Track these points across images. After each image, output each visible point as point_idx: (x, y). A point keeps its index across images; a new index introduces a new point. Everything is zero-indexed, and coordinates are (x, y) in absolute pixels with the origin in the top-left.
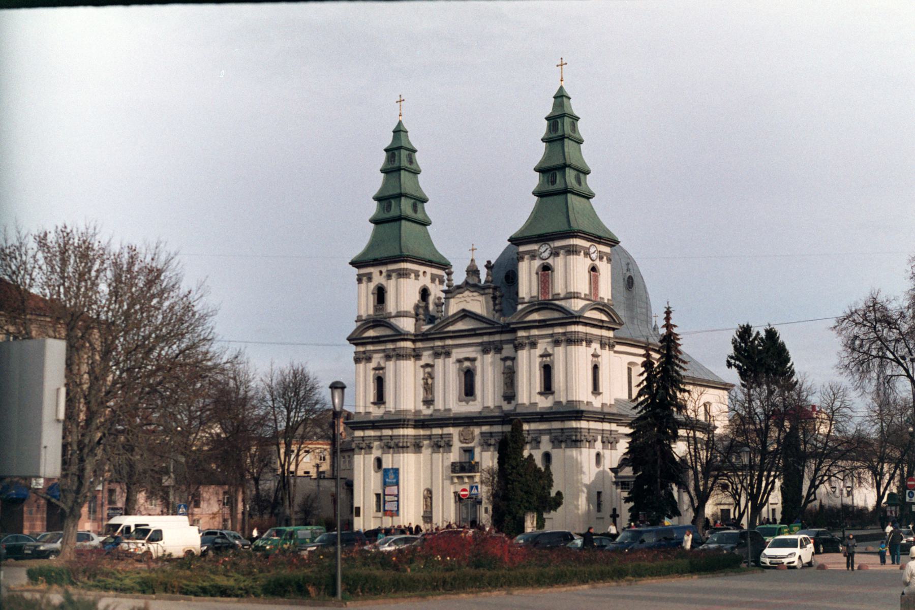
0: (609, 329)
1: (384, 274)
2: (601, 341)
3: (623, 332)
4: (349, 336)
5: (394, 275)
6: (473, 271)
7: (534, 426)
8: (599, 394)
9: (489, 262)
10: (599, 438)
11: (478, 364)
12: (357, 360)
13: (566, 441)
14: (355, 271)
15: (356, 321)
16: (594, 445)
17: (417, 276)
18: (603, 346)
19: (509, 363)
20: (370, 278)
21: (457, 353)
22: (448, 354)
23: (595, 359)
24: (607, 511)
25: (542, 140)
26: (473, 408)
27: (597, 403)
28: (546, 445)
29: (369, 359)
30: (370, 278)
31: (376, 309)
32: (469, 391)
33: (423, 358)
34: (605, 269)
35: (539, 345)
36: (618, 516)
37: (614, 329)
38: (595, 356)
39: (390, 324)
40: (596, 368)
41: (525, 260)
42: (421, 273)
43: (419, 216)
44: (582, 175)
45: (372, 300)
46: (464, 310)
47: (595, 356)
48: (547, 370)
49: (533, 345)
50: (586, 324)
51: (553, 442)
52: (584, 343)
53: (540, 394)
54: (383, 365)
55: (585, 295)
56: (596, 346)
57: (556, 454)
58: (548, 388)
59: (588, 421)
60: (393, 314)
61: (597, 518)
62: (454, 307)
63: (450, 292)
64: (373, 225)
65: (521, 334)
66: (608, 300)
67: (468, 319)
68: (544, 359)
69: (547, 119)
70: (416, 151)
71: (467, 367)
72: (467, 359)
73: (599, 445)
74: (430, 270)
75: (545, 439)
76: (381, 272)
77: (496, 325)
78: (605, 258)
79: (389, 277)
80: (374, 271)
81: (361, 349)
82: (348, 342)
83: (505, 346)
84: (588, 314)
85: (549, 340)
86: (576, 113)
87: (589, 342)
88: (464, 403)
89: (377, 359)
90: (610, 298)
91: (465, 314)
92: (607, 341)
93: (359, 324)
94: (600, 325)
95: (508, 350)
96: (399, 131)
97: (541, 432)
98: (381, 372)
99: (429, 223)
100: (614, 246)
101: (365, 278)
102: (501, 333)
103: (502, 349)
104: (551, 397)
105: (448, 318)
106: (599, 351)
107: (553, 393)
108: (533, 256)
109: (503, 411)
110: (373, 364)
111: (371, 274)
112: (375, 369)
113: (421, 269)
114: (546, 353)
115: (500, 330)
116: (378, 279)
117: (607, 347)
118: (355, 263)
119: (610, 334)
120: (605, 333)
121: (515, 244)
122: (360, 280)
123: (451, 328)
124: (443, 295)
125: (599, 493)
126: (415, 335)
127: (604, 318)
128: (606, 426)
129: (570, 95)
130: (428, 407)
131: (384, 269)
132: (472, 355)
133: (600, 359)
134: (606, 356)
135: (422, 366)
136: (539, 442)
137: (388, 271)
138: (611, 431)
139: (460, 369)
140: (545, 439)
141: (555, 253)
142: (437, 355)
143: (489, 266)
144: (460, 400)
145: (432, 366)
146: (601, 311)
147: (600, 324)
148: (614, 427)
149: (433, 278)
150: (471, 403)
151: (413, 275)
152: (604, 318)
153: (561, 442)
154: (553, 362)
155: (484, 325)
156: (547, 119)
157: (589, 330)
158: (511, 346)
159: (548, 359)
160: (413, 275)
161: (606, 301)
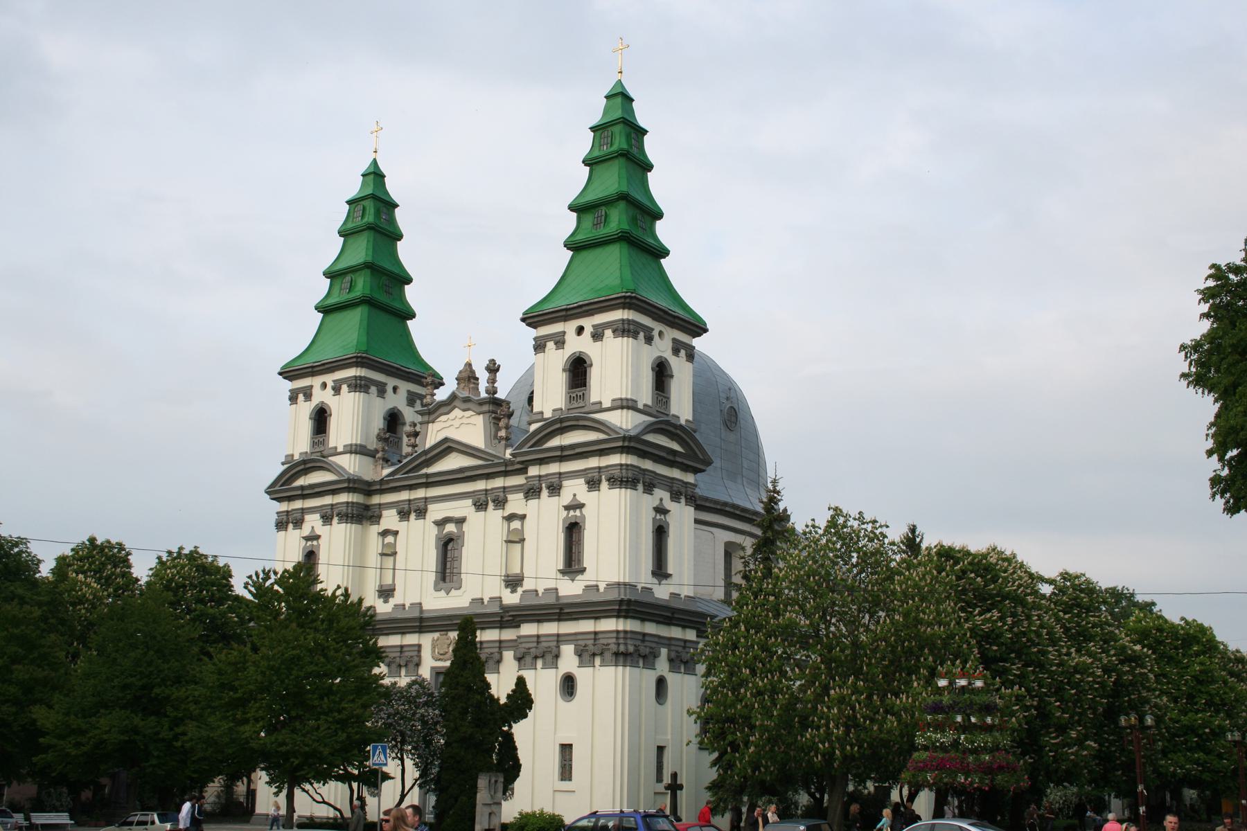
0: (686, 468)
1: (330, 384)
2: (671, 487)
3: (707, 484)
4: (269, 488)
5: (345, 388)
6: (468, 377)
7: (550, 628)
8: (668, 576)
9: (493, 361)
10: (664, 651)
11: (465, 527)
12: (281, 525)
13: (601, 654)
14: (289, 385)
15: (283, 464)
16: (653, 664)
17: (382, 392)
18: (675, 497)
19: (516, 524)
20: (308, 396)
21: (437, 511)
22: (422, 513)
23: (658, 517)
24: (667, 779)
25: (583, 162)
26: (457, 601)
27: (662, 592)
28: (568, 660)
29: (298, 523)
30: (308, 396)
31: (314, 444)
32: (447, 572)
33: (382, 521)
34: (682, 372)
35: (563, 492)
36: (681, 787)
37: (696, 471)
38: (661, 510)
39: (330, 465)
40: (660, 533)
41: (546, 350)
42: (389, 389)
43: (397, 305)
44: (648, 219)
45: (306, 427)
46: (446, 440)
47: (661, 510)
48: (573, 530)
49: (555, 489)
50: (643, 454)
51: (580, 656)
52: (640, 487)
53: (563, 572)
54: (318, 533)
55: (645, 405)
56: (661, 495)
57: (583, 676)
58: (572, 564)
59: (643, 620)
60: (340, 449)
61: (655, 793)
62: (434, 434)
63: (433, 411)
64: (321, 315)
65: (533, 471)
66: (687, 421)
67: (454, 455)
68: (572, 513)
69: (590, 128)
70: (397, 206)
71: (450, 533)
72: (447, 520)
73: (662, 666)
74: (405, 387)
75: (568, 650)
76: (324, 385)
77: (496, 461)
78: (683, 353)
79: (337, 390)
80: (316, 382)
81: (284, 507)
82: (268, 497)
83: (510, 497)
84: (651, 438)
85: (582, 481)
86: (642, 122)
87: (649, 489)
88: (443, 593)
89: (313, 522)
90: (691, 419)
91: (447, 447)
92: (683, 490)
93: (286, 466)
94: (668, 459)
95: (516, 503)
96: (375, 175)
97: (560, 639)
98: (315, 543)
99: (412, 316)
100: (699, 335)
101: (301, 397)
102: (506, 474)
103: (505, 501)
104: (580, 577)
105: (425, 452)
106: (668, 504)
107: (583, 571)
108: (560, 342)
109: (502, 607)
110: (306, 530)
111: (311, 387)
112: (307, 539)
113: (391, 382)
114: (574, 503)
115: (503, 469)
116: (319, 396)
117: (683, 500)
118: (289, 373)
119: (690, 478)
120: (676, 473)
121: (529, 325)
122: (293, 399)
123: (424, 471)
124: (419, 418)
125: (661, 749)
126: (369, 484)
127: (675, 446)
128: (676, 632)
129: (632, 95)
130: (386, 601)
131: (329, 379)
132: (457, 514)
133: (667, 516)
134: (682, 516)
135: (379, 533)
136: (557, 656)
137: (334, 381)
138: (685, 641)
139: (438, 538)
140: (568, 650)
141: (597, 336)
142: (404, 515)
143: (493, 369)
144: (437, 589)
145: (396, 533)
146: (672, 436)
147: (671, 458)
148: (691, 635)
149: (412, 399)
150: (453, 592)
151: (373, 389)
152: (675, 446)
153: (594, 655)
154: (583, 517)
155: (480, 462)
156: (590, 128)
157: (648, 465)
158: (521, 495)
159: (578, 513)
160: (373, 389)
161: (683, 422)
